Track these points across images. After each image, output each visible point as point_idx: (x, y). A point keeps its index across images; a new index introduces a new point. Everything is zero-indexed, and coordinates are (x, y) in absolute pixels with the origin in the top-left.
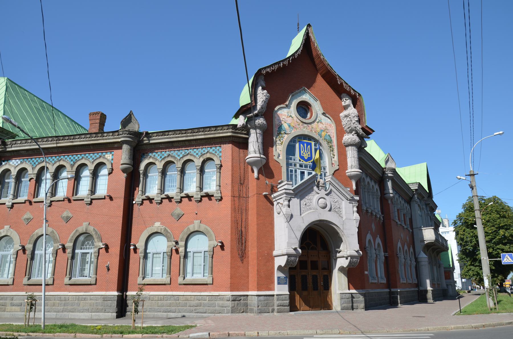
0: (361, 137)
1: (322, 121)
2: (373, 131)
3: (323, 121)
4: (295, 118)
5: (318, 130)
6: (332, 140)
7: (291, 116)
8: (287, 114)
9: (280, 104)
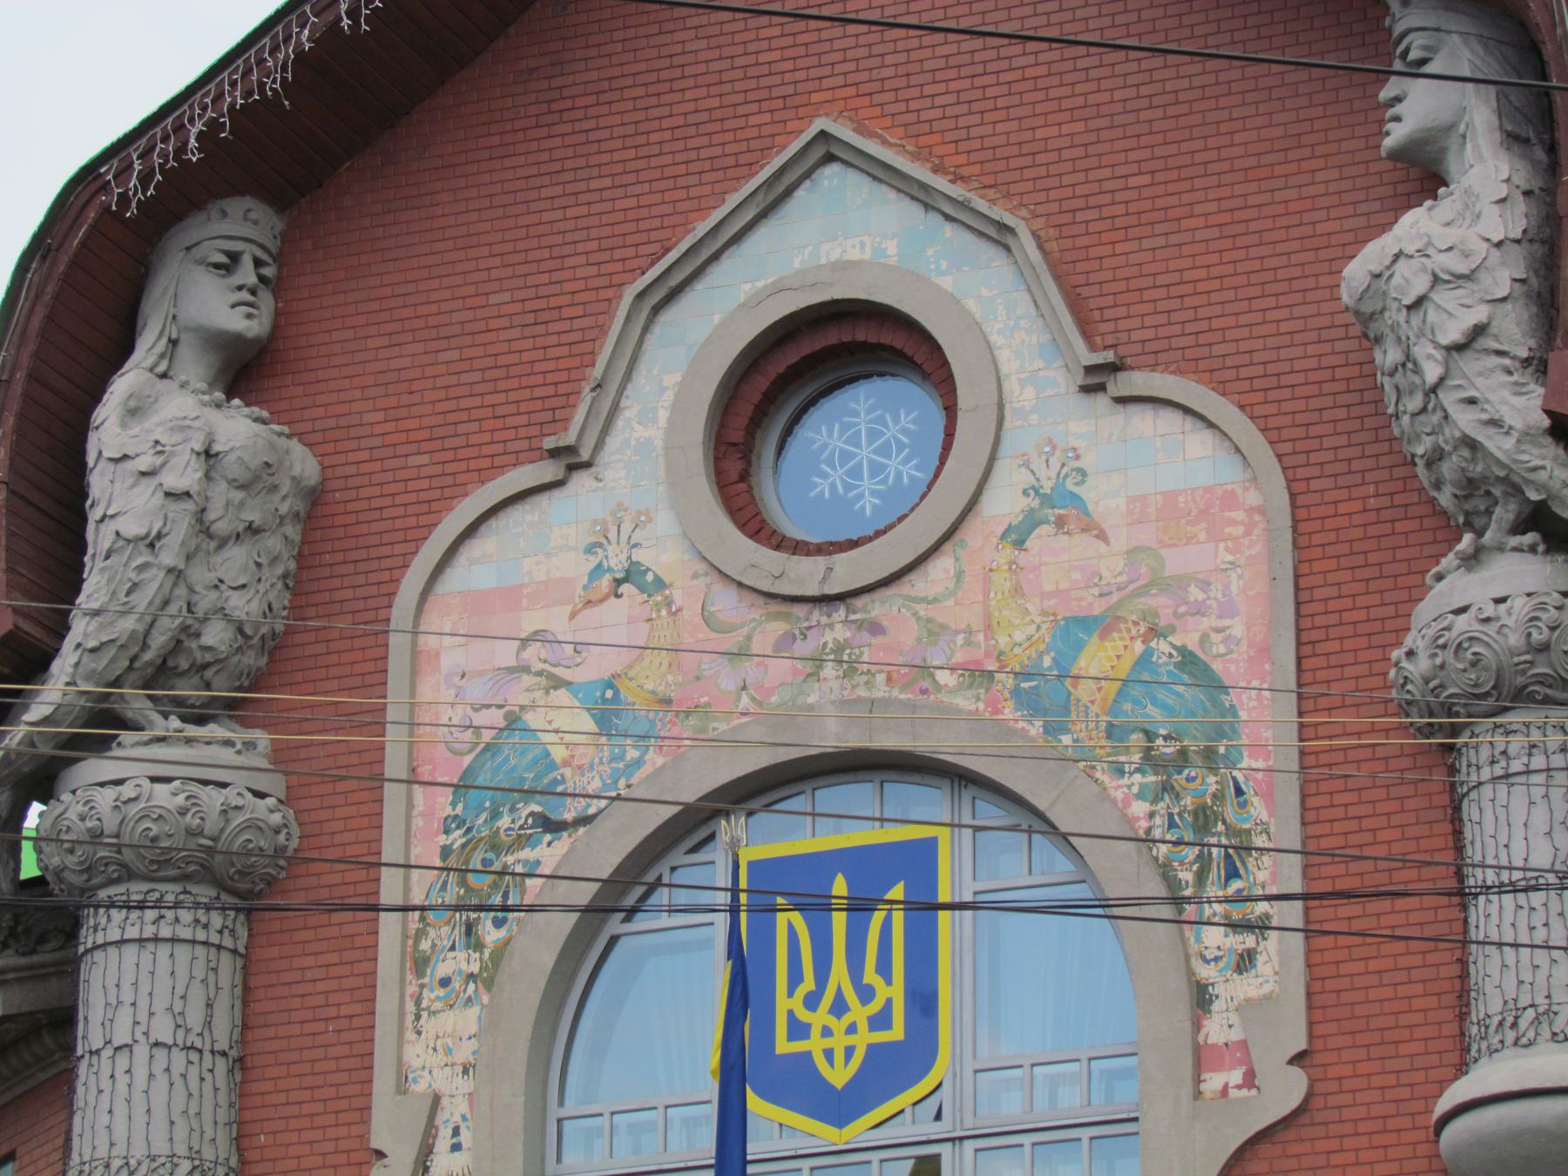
1: (1087, 492)
3: (1104, 496)
4: (688, 587)
5: (1021, 633)
7: (632, 574)
8: (575, 566)
9: (485, 475)
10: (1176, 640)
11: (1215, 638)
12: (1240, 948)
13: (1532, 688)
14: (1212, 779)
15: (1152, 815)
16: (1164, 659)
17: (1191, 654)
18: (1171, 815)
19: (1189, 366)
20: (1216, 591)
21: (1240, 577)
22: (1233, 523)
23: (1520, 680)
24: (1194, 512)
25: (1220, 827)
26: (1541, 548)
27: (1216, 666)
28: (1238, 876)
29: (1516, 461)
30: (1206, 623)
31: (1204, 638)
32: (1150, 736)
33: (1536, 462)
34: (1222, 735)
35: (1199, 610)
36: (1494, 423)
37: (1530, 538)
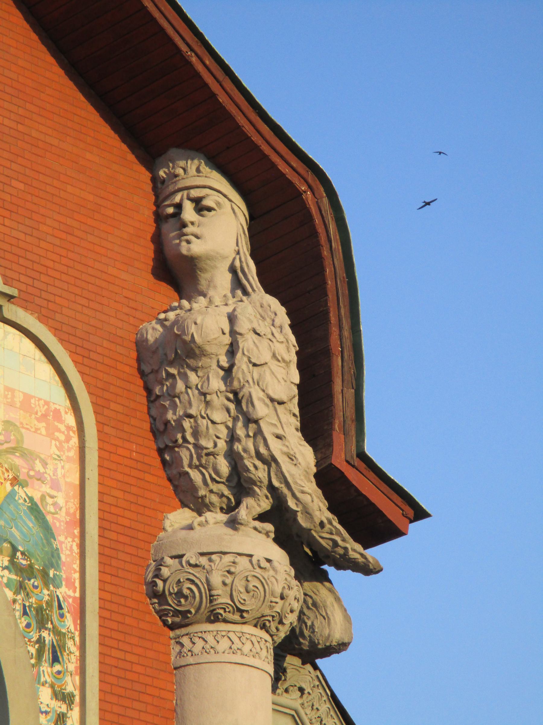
0: (310, 561)
2: (420, 514)
6: (53, 558)
10: (30, 492)
11: (49, 501)
12: (59, 710)
13: (218, 611)
14: (46, 592)
15: (14, 601)
16: (21, 501)
17: (36, 504)
18: (24, 606)
19: (43, 319)
20: (50, 470)
21: (63, 467)
22: (59, 431)
23: (267, 612)
24: (39, 414)
25: (50, 626)
26: (272, 535)
27: (49, 518)
28: (58, 662)
29: (296, 483)
30: (46, 489)
31: (43, 498)
32: (15, 550)
33: (306, 489)
34: (52, 566)
35: (40, 478)
36: (291, 458)
37: (269, 527)
